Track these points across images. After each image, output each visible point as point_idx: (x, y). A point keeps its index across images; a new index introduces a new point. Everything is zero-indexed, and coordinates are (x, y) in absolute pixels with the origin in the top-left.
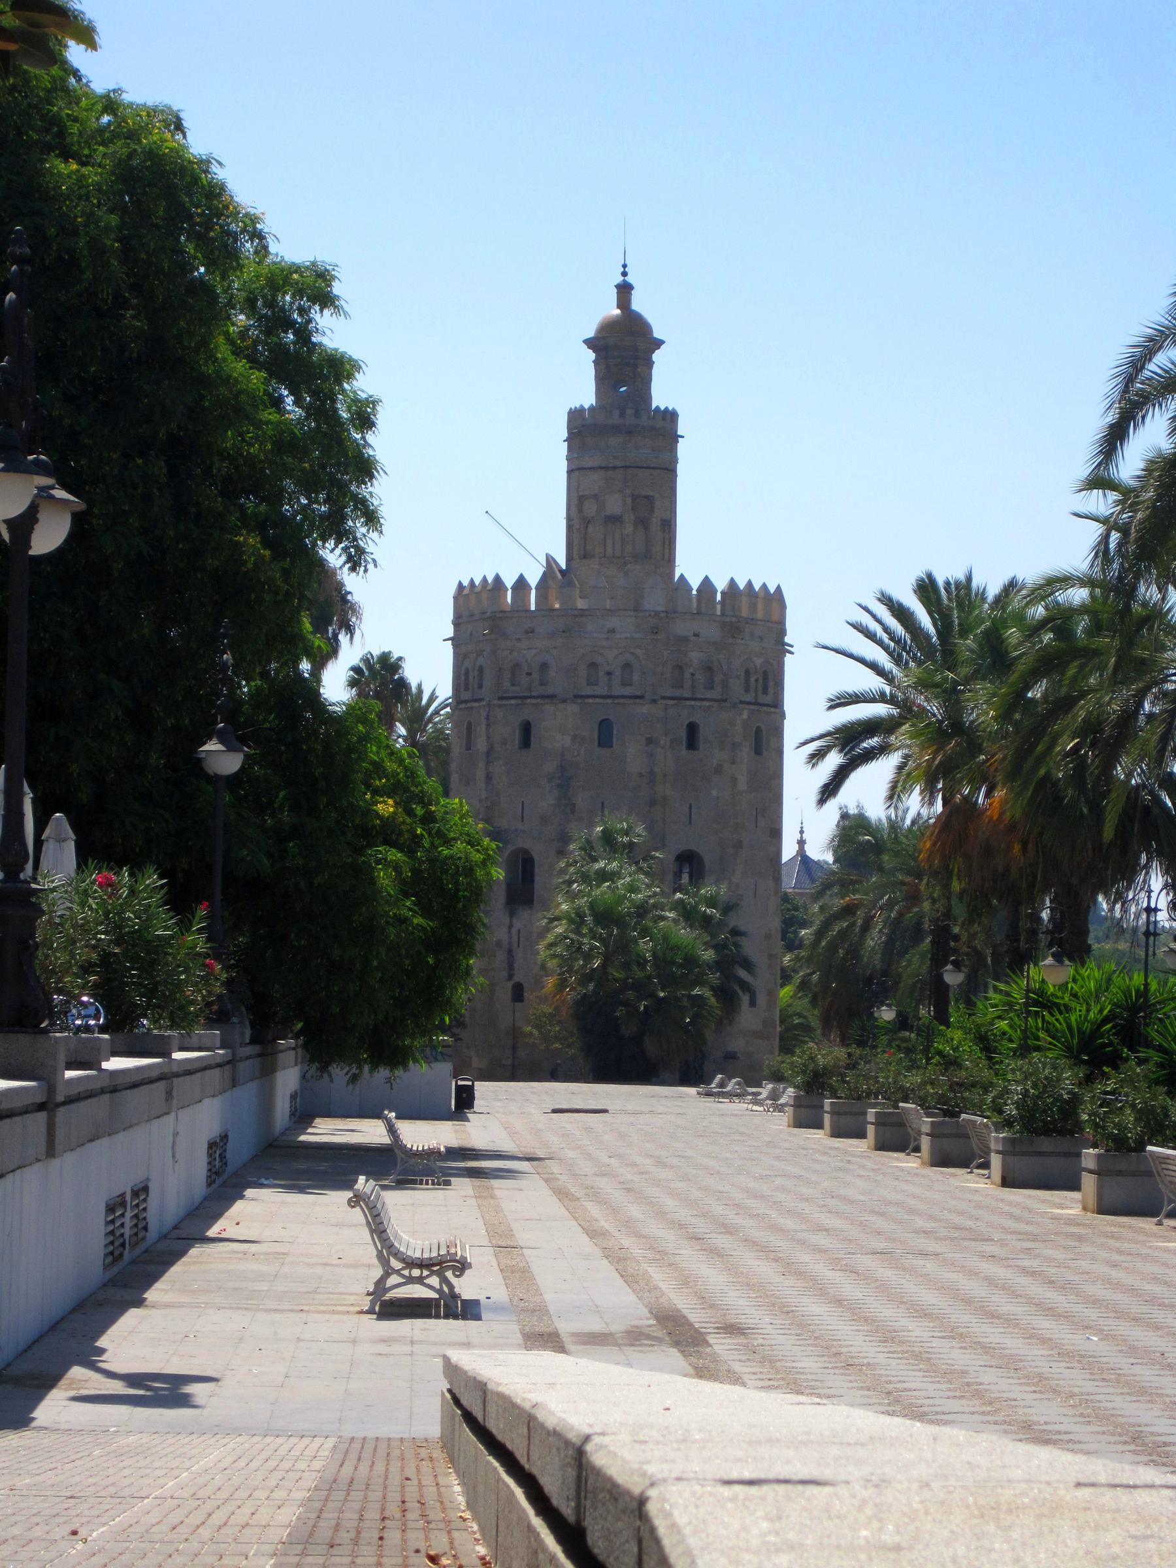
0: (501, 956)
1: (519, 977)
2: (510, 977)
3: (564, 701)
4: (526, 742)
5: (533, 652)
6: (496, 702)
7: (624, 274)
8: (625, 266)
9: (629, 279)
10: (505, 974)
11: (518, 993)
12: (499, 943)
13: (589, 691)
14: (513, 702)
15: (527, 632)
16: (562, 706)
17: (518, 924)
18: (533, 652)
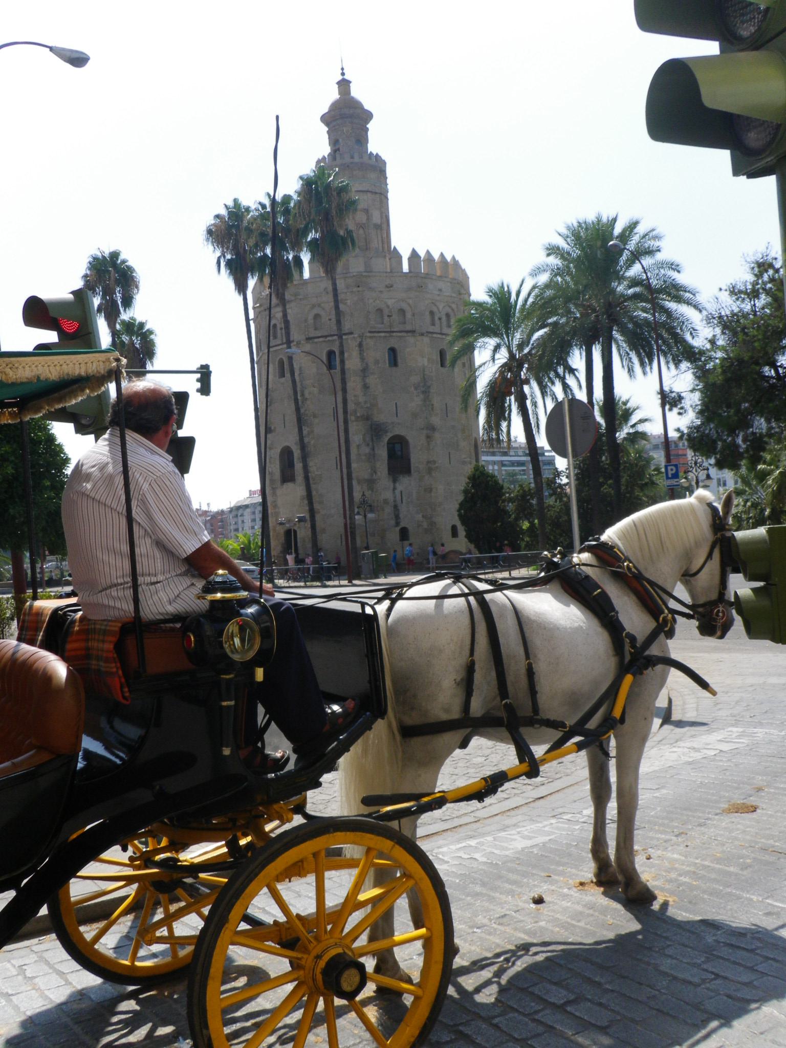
0: (389, 510)
1: (402, 525)
2: (397, 524)
3: (422, 335)
4: (394, 362)
5: (393, 301)
6: (369, 334)
7: (343, 74)
8: (342, 69)
9: (346, 77)
10: (393, 522)
11: (404, 534)
12: (386, 502)
13: (431, 329)
14: (383, 334)
15: (387, 287)
16: (419, 338)
17: (400, 487)
18: (393, 301)
